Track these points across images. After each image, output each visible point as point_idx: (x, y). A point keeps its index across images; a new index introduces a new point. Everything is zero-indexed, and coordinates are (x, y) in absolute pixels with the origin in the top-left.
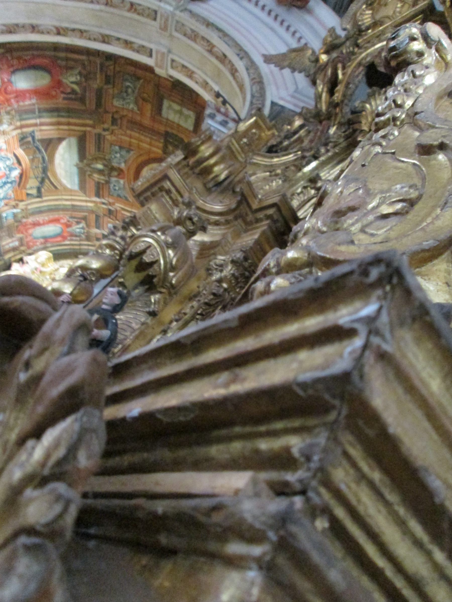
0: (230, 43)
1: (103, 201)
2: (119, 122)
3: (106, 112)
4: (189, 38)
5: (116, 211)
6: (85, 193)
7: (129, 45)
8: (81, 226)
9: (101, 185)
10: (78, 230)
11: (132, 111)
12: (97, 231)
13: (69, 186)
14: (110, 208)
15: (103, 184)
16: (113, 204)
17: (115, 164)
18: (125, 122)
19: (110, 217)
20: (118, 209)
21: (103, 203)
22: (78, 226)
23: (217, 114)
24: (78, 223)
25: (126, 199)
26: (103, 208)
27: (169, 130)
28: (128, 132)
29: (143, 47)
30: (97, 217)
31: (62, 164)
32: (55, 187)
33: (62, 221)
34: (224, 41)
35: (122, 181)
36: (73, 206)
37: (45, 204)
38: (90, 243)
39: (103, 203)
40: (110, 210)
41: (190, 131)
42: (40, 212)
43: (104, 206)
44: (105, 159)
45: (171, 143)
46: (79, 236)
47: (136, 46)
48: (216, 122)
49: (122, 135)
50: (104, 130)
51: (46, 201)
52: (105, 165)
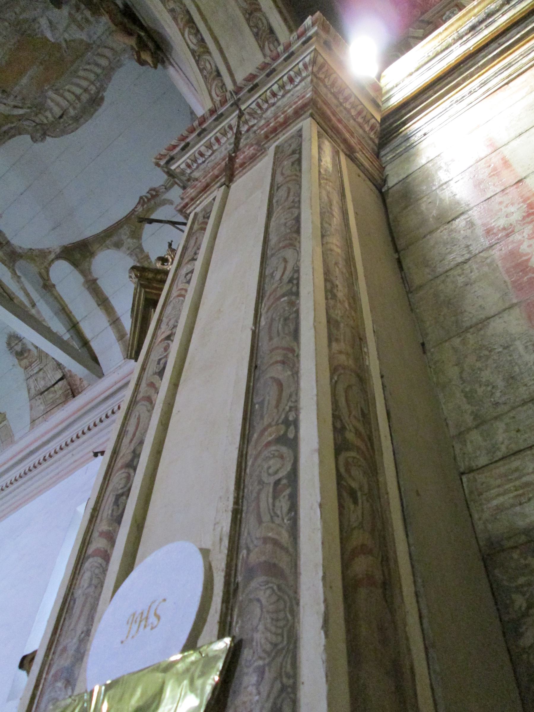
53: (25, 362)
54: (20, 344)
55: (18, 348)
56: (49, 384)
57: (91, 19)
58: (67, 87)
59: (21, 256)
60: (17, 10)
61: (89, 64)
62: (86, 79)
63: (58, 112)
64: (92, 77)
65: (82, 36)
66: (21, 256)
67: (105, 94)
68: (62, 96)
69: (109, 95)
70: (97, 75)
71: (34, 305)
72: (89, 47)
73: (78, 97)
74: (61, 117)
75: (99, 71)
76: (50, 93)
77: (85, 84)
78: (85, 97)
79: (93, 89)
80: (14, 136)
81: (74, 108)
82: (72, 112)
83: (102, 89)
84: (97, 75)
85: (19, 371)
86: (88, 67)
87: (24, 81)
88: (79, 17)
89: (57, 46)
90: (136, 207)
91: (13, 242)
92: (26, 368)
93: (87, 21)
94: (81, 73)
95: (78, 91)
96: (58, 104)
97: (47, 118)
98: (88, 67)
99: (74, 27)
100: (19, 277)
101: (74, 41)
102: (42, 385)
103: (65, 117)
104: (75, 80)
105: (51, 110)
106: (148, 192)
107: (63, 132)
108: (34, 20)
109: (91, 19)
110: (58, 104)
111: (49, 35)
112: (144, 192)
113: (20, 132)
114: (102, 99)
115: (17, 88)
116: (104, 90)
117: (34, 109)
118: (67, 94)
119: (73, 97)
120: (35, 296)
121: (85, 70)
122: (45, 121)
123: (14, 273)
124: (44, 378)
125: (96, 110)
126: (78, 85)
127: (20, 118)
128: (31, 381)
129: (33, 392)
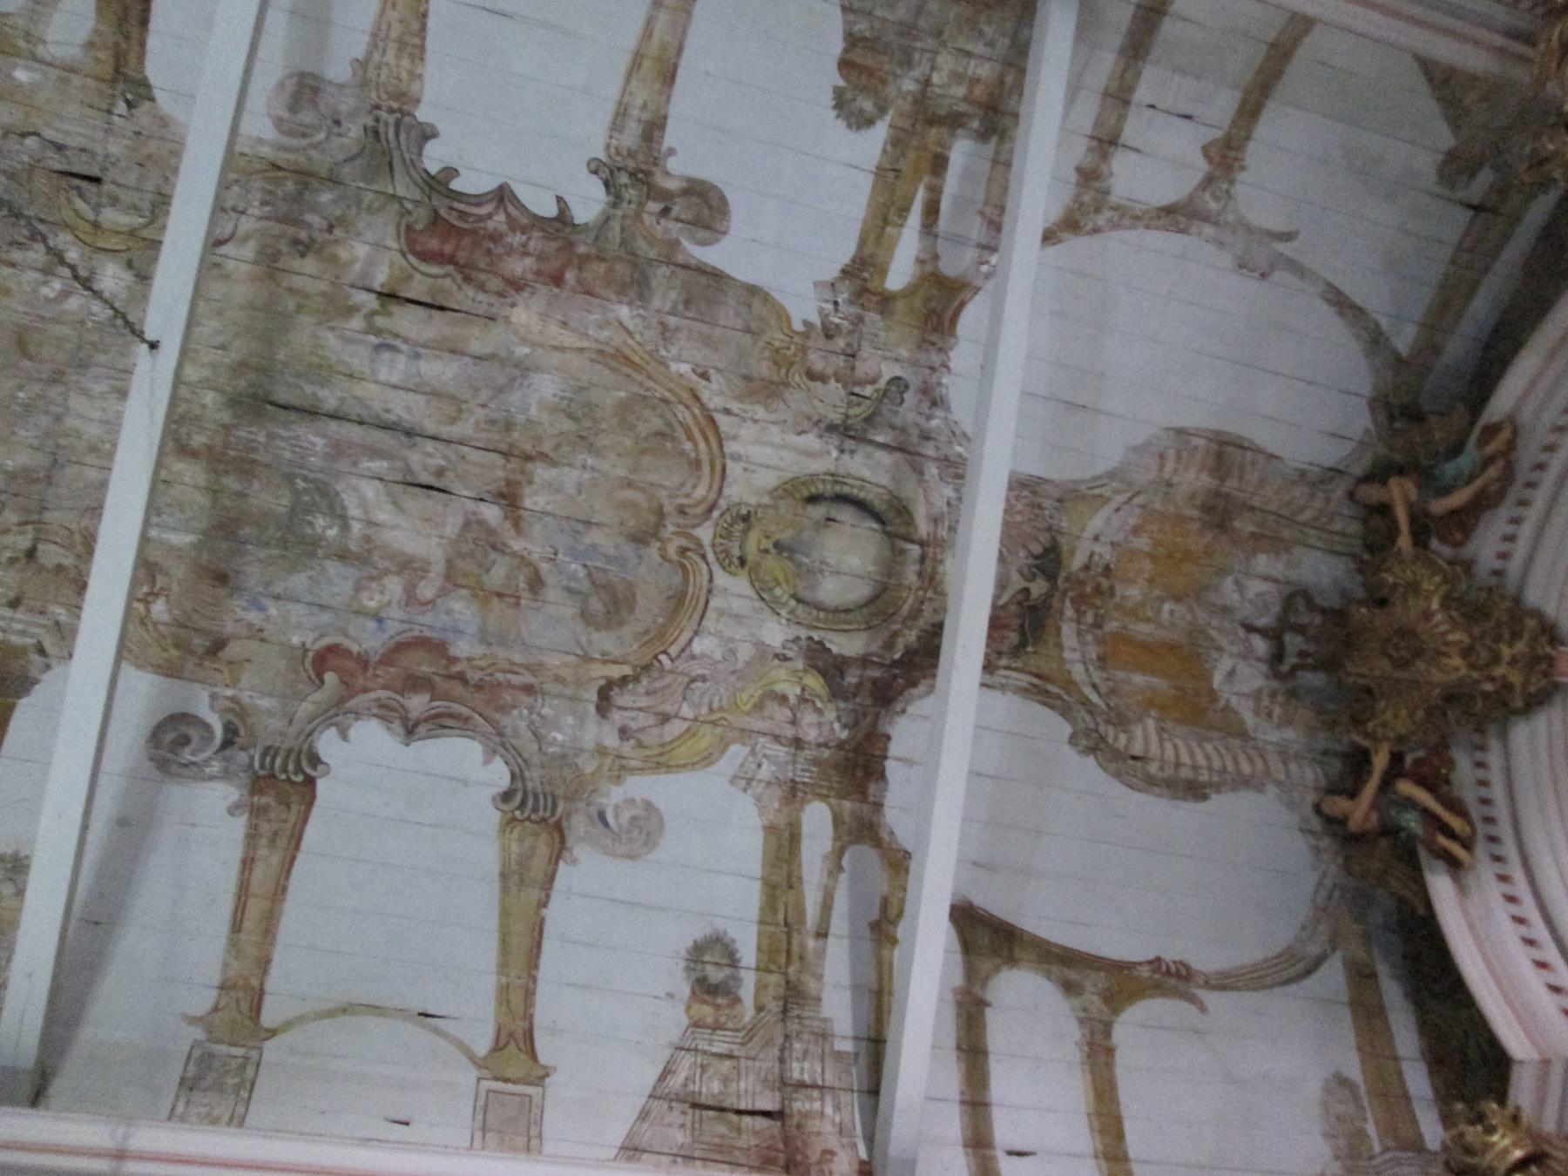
53: (706, 1012)
54: (727, 971)
55: (715, 975)
56: (731, 1102)
57: (1275, 719)
58: (1177, 741)
59: (877, 842)
60: (1215, 622)
61: (1227, 748)
62: (1208, 757)
63: (1137, 749)
64: (1217, 764)
65: (1249, 719)
66: (877, 842)
67: (1214, 796)
68: (1161, 740)
69: (1217, 802)
70: (1224, 770)
71: (822, 934)
72: (1243, 735)
73: (1178, 765)
74: (1134, 758)
75: (1230, 768)
76: (1151, 723)
77: (1201, 760)
78: (1186, 773)
79: (1204, 777)
80: (1052, 707)
81: (1161, 769)
82: (1153, 768)
83: (1218, 788)
84: (1224, 770)
85: (673, 1020)
86: (1223, 751)
87: (1138, 679)
88: (1266, 702)
89: (1213, 695)
90: (1140, 964)
91: (887, 810)
92: (696, 1024)
93: (1270, 715)
94: (1209, 747)
95: (1185, 759)
96: (1146, 738)
97: (1116, 739)
98: (1223, 751)
99: (1251, 704)
100: (840, 868)
101: (1236, 713)
102: (710, 1088)
103: (1139, 764)
104: (1194, 745)
105: (1130, 739)
106: (1174, 962)
107: (1117, 775)
108: (1220, 649)
109: (1275, 719)
110: (1146, 738)
111: (1217, 680)
112: (1170, 955)
113: (1065, 712)
114: (1205, 798)
115: (1120, 674)
116: (1218, 791)
117: (1113, 714)
118: (1168, 746)
119: (1172, 759)
120: (839, 923)
121: (1216, 749)
122: (1110, 740)
123: (839, 853)
124: (726, 1081)
125: (1185, 799)
126: (1192, 755)
127: (1086, 702)
128: (687, 1061)
129: (676, 1082)
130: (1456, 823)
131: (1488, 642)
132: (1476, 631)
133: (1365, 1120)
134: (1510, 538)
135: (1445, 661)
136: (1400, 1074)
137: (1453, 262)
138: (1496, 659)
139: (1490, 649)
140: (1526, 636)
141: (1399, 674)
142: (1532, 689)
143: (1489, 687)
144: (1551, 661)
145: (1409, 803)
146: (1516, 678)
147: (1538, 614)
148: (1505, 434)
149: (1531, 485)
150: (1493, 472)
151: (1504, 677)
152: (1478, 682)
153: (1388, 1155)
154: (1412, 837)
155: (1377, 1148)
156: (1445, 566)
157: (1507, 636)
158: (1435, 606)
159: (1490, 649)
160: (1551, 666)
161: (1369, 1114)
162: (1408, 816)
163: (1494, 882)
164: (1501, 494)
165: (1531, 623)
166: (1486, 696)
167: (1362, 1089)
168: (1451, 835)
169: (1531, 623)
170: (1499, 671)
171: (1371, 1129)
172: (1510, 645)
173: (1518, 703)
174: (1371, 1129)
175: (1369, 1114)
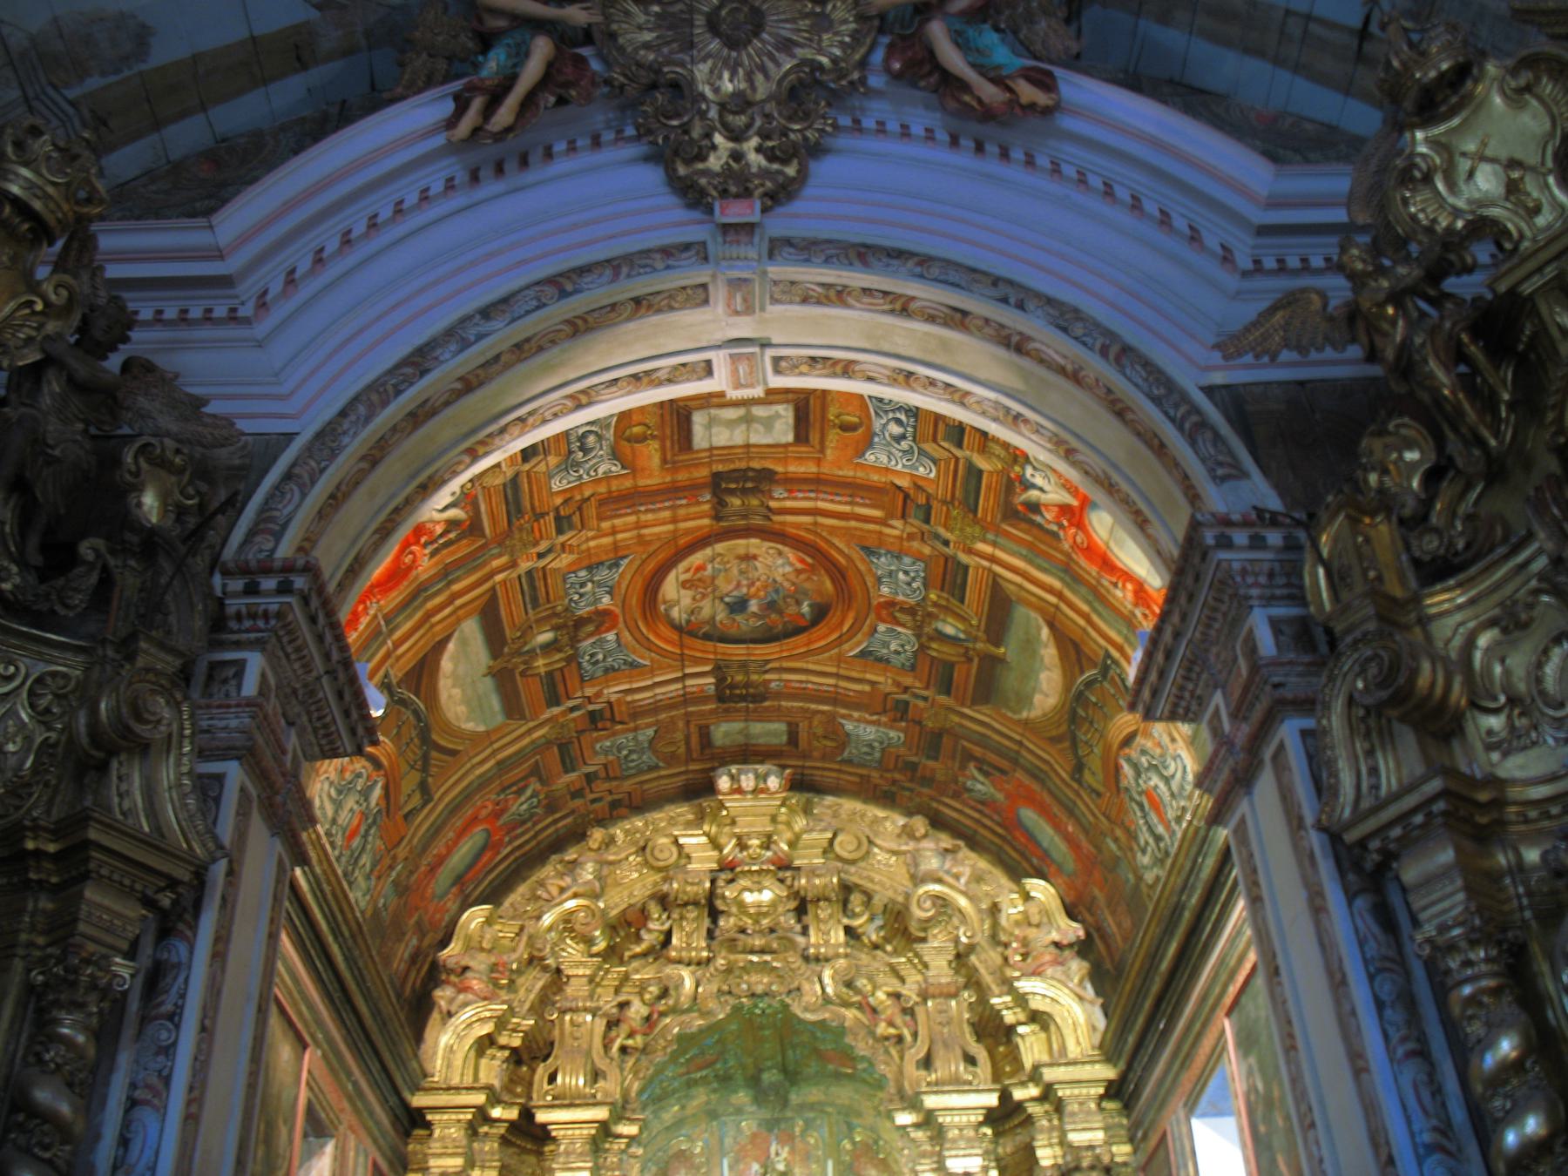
0: (953, 276)
1: (571, 704)
2: (576, 519)
3: (539, 516)
4: (819, 303)
5: (610, 704)
6: (523, 717)
7: (645, 380)
8: (529, 793)
9: (558, 675)
10: (525, 807)
11: (608, 478)
12: (573, 776)
13: (482, 728)
14: (591, 707)
15: (561, 669)
16: (598, 694)
17: (584, 610)
18: (591, 510)
19: (597, 729)
20: (613, 698)
21: (572, 709)
22: (523, 799)
23: (1229, 531)
24: (520, 792)
25: (633, 665)
26: (574, 720)
27: (720, 468)
28: (606, 525)
29: (684, 365)
30: (564, 748)
31: (456, 692)
32: (453, 753)
33: (484, 813)
34: (936, 280)
35: (611, 636)
36: (499, 763)
37: (441, 807)
38: (557, 815)
39: (572, 709)
40: (592, 714)
41: (786, 446)
42: (436, 831)
43: (576, 714)
44: (556, 615)
45: (732, 492)
46: (532, 816)
47: (662, 375)
48: (1241, 549)
49: (588, 540)
50: (540, 556)
51: (441, 799)
52: (555, 628)
130: (505, 114)
131: (758, 123)
132: (771, 107)
133: (103, 74)
134: (905, 132)
135: (726, 75)
136: (183, 115)
137: (1288, 12)
138: (736, 136)
139: (749, 126)
140: (775, 166)
141: (700, 20)
142: (703, 181)
143: (696, 132)
144: (746, 193)
145: (522, 54)
146: (715, 162)
147: (803, 174)
148: (1042, 98)
149: (980, 148)
150: (990, 92)
151: (714, 147)
152: (703, 115)
153: (71, 111)
154: (477, 66)
155: (72, 94)
156: (857, 57)
157: (770, 144)
158: (801, 52)
159: (749, 126)
160: (737, 196)
161: (112, 79)
162: (503, 57)
163: (444, 175)
164: (966, 112)
165: (791, 171)
166: (685, 128)
167: (144, 67)
168: (489, 110)
169: (791, 171)
170: (718, 139)
171: (94, 82)
172: (759, 150)
173: (682, 170)
174: (94, 82)
175: (112, 79)
